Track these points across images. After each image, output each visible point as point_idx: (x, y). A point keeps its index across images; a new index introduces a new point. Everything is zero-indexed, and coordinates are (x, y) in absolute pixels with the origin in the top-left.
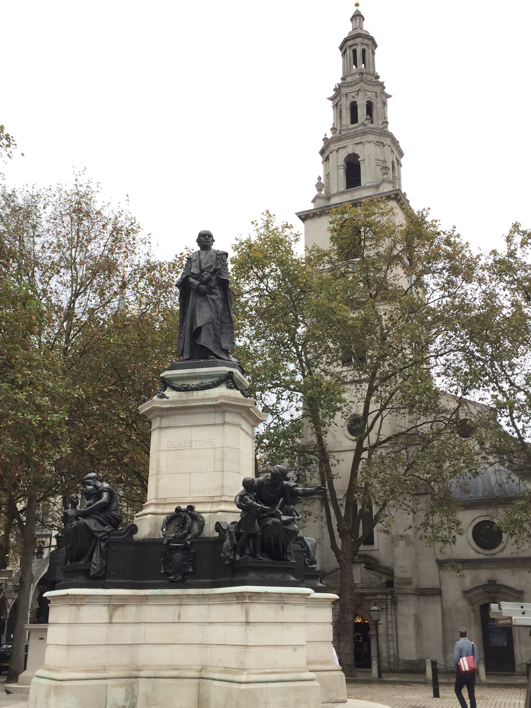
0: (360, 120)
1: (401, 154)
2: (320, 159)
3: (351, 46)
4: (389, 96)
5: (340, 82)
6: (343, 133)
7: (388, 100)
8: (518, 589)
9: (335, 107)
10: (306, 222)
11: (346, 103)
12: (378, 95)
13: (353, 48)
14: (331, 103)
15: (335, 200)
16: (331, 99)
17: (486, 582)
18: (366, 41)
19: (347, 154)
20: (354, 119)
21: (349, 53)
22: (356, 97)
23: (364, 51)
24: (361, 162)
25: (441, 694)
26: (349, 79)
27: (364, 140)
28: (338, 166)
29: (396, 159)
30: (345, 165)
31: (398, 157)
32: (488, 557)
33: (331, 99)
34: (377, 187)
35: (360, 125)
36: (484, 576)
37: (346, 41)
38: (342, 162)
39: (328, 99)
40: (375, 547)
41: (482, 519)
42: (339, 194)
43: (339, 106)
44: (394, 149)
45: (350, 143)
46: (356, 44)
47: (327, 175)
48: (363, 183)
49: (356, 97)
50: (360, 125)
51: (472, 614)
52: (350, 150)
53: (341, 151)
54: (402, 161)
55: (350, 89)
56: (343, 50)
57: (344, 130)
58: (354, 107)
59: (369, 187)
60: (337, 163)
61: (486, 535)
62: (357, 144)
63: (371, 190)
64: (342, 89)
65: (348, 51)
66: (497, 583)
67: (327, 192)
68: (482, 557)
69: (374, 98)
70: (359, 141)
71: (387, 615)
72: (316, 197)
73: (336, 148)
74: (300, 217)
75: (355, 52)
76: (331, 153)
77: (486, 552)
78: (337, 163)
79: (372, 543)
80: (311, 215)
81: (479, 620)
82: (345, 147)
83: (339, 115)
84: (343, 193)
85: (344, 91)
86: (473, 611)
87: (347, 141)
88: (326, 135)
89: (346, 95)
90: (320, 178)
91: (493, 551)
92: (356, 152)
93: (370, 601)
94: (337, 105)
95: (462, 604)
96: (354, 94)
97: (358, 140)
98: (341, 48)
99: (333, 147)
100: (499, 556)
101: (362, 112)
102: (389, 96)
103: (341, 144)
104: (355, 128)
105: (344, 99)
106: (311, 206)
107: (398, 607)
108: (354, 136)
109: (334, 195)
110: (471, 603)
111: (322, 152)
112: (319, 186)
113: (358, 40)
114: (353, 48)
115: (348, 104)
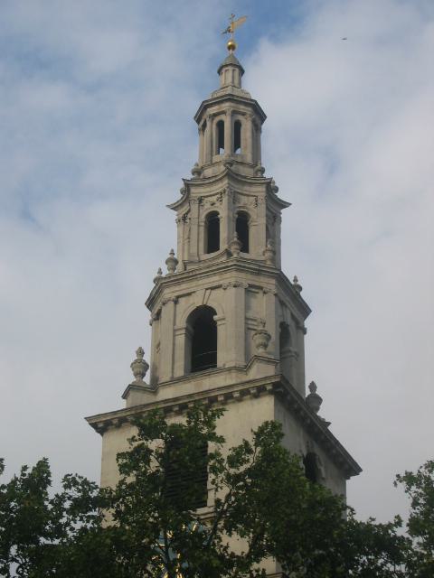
0: (223, 246)
1: (305, 311)
2: (147, 315)
4: (284, 205)
5: (189, 176)
6: (189, 268)
7: (283, 211)
9: (182, 222)
10: (105, 435)
11: (199, 215)
12: (260, 201)
13: (217, 119)
14: (174, 215)
15: (166, 394)
16: (175, 207)
18: (242, 108)
19: (193, 308)
20: (212, 245)
21: (211, 128)
22: (218, 204)
24: (219, 323)
26: (208, 172)
28: (175, 331)
29: (293, 316)
30: (191, 329)
31: (297, 314)
33: (175, 207)
34: (245, 369)
35: (222, 255)
37: (205, 106)
38: (182, 322)
39: (168, 206)
42: (174, 381)
43: (188, 221)
44: (287, 299)
45: (199, 288)
46: (224, 113)
47: (157, 346)
48: (219, 364)
49: (218, 204)
50: (222, 255)
52: (196, 301)
53: (182, 301)
54: (308, 323)
55: (208, 189)
56: (202, 123)
57: (191, 262)
58: (212, 221)
59: (229, 370)
60: (174, 324)
62: (212, 289)
63: (234, 374)
64: (193, 190)
65: (208, 123)
67: (154, 379)
69: (252, 207)
70: (215, 285)
72: (131, 388)
73: (173, 296)
74: (94, 425)
75: (221, 125)
76: (164, 304)
78: (174, 324)
80: (115, 422)
82: (189, 294)
83: (186, 239)
84: (180, 380)
85: (196, 192)
87: (194, 284)
88: (160, 272)
89: (200, 200)
90: (141, 352)
92: (210, 304)
94: (184, 218)
97: (215, 280)
98: (198, 119)
99: (169, 293)
102: (284, 205)
103: (184, 287)
104: (214, 258)
105: (195, 207)
106: (122, 404)
108: (207, 274)
109: (166, 384)
111: (151, 303)
112: (140, 367)
113: (226, 106)
114: (217, 119)
115: (203, 217)
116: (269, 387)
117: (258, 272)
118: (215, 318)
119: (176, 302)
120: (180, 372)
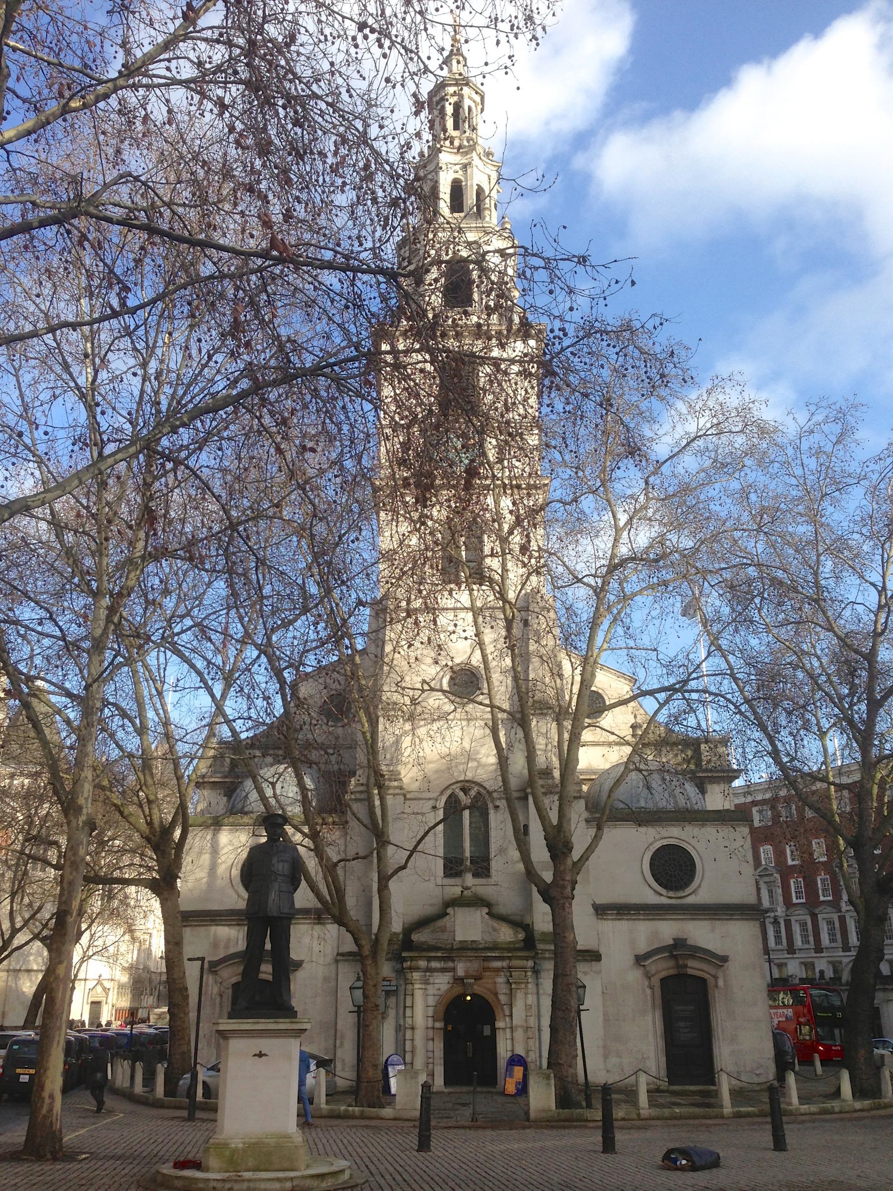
8: (720, 952)
17: (671, 942)
22: (461, 172)
25: (790, 1139)
32: (673, 901)
36: (667, 930)
40: (492, 881)
41: (665, 842)
51: (648, 991)
61: (674, 868)
66: (689, 942)
68: (664, 901)
71: (526, 994)
77: (671, 894)
79: (488, 876)
81: (659, 1001)
86: (651, 987)
91: (681, 894)
93: (498, 970)
95: (635, 976)
100: (691, 900)
101: (470, 199)
107: (541, 981)
110: (648, 976)
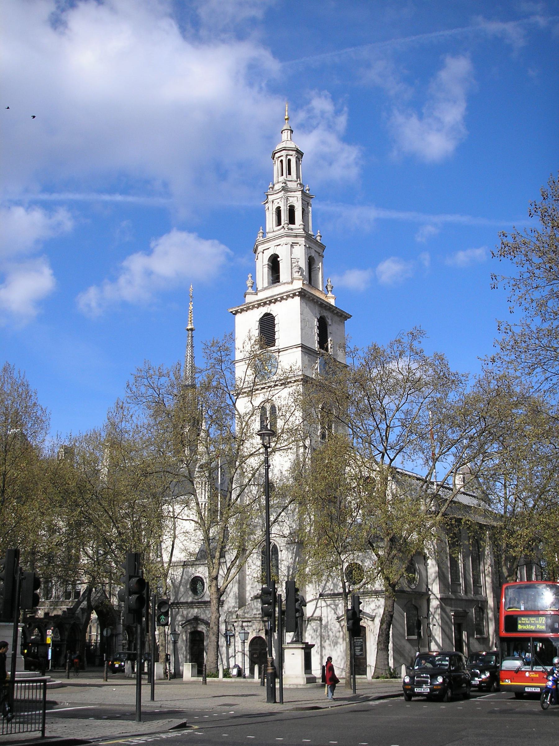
3: (279, 157)
13: (280, 159)
18: (291, 153)
23: (289, 161)
27: (282, 243)
42: (264, 289)
46: (282, 156)
49: (280, 203)
59: (284, 284)
75: (281, 161)
87: (270, 243)
96: (278, 200)
97: (277, 242)
113: (284, 153)
115: (274, 210)
116: (297, 293)
117: (296, 236)
118: (279, 259)
119: (263, 253)
120: (266, 285)
